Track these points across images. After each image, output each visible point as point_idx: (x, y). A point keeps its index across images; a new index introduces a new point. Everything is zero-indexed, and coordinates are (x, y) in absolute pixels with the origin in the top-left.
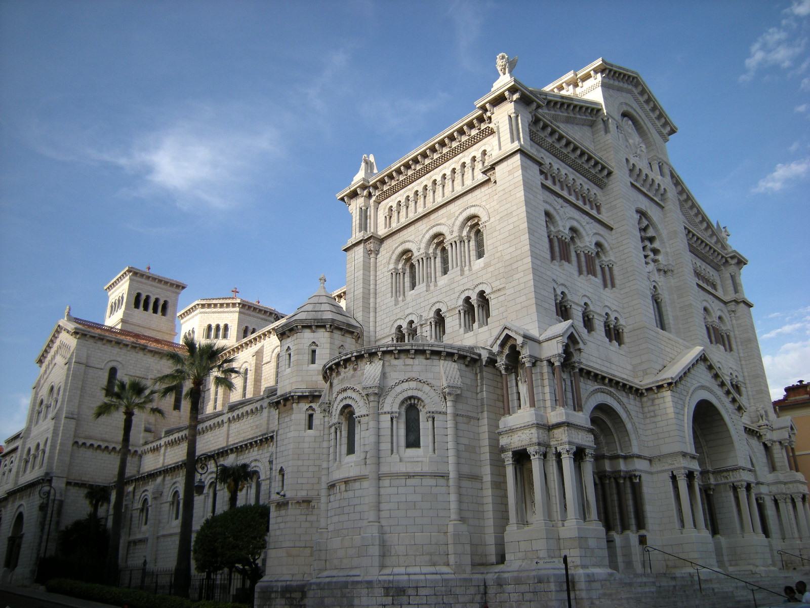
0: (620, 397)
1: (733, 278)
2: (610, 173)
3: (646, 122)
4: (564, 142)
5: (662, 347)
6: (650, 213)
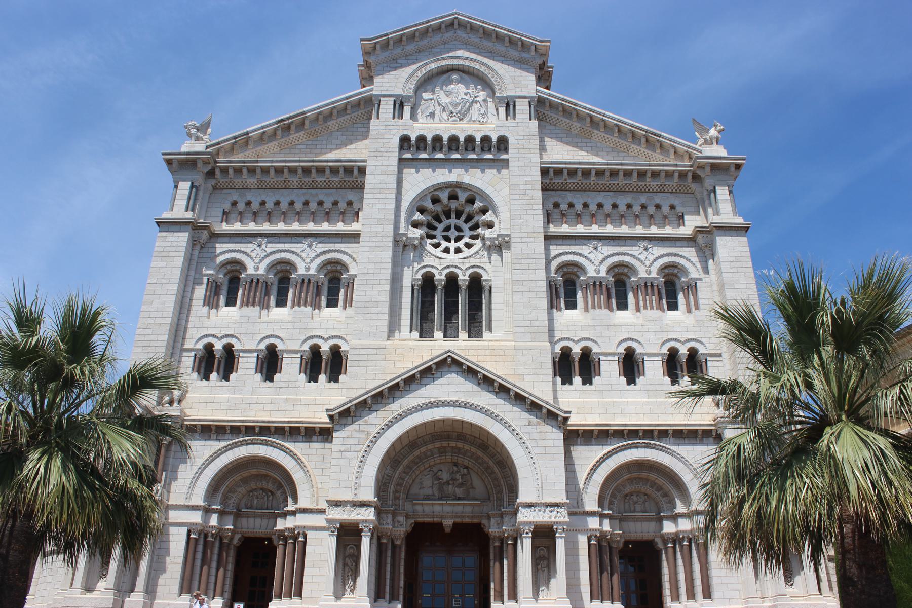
2: (362, 171)
4: (272, 172)
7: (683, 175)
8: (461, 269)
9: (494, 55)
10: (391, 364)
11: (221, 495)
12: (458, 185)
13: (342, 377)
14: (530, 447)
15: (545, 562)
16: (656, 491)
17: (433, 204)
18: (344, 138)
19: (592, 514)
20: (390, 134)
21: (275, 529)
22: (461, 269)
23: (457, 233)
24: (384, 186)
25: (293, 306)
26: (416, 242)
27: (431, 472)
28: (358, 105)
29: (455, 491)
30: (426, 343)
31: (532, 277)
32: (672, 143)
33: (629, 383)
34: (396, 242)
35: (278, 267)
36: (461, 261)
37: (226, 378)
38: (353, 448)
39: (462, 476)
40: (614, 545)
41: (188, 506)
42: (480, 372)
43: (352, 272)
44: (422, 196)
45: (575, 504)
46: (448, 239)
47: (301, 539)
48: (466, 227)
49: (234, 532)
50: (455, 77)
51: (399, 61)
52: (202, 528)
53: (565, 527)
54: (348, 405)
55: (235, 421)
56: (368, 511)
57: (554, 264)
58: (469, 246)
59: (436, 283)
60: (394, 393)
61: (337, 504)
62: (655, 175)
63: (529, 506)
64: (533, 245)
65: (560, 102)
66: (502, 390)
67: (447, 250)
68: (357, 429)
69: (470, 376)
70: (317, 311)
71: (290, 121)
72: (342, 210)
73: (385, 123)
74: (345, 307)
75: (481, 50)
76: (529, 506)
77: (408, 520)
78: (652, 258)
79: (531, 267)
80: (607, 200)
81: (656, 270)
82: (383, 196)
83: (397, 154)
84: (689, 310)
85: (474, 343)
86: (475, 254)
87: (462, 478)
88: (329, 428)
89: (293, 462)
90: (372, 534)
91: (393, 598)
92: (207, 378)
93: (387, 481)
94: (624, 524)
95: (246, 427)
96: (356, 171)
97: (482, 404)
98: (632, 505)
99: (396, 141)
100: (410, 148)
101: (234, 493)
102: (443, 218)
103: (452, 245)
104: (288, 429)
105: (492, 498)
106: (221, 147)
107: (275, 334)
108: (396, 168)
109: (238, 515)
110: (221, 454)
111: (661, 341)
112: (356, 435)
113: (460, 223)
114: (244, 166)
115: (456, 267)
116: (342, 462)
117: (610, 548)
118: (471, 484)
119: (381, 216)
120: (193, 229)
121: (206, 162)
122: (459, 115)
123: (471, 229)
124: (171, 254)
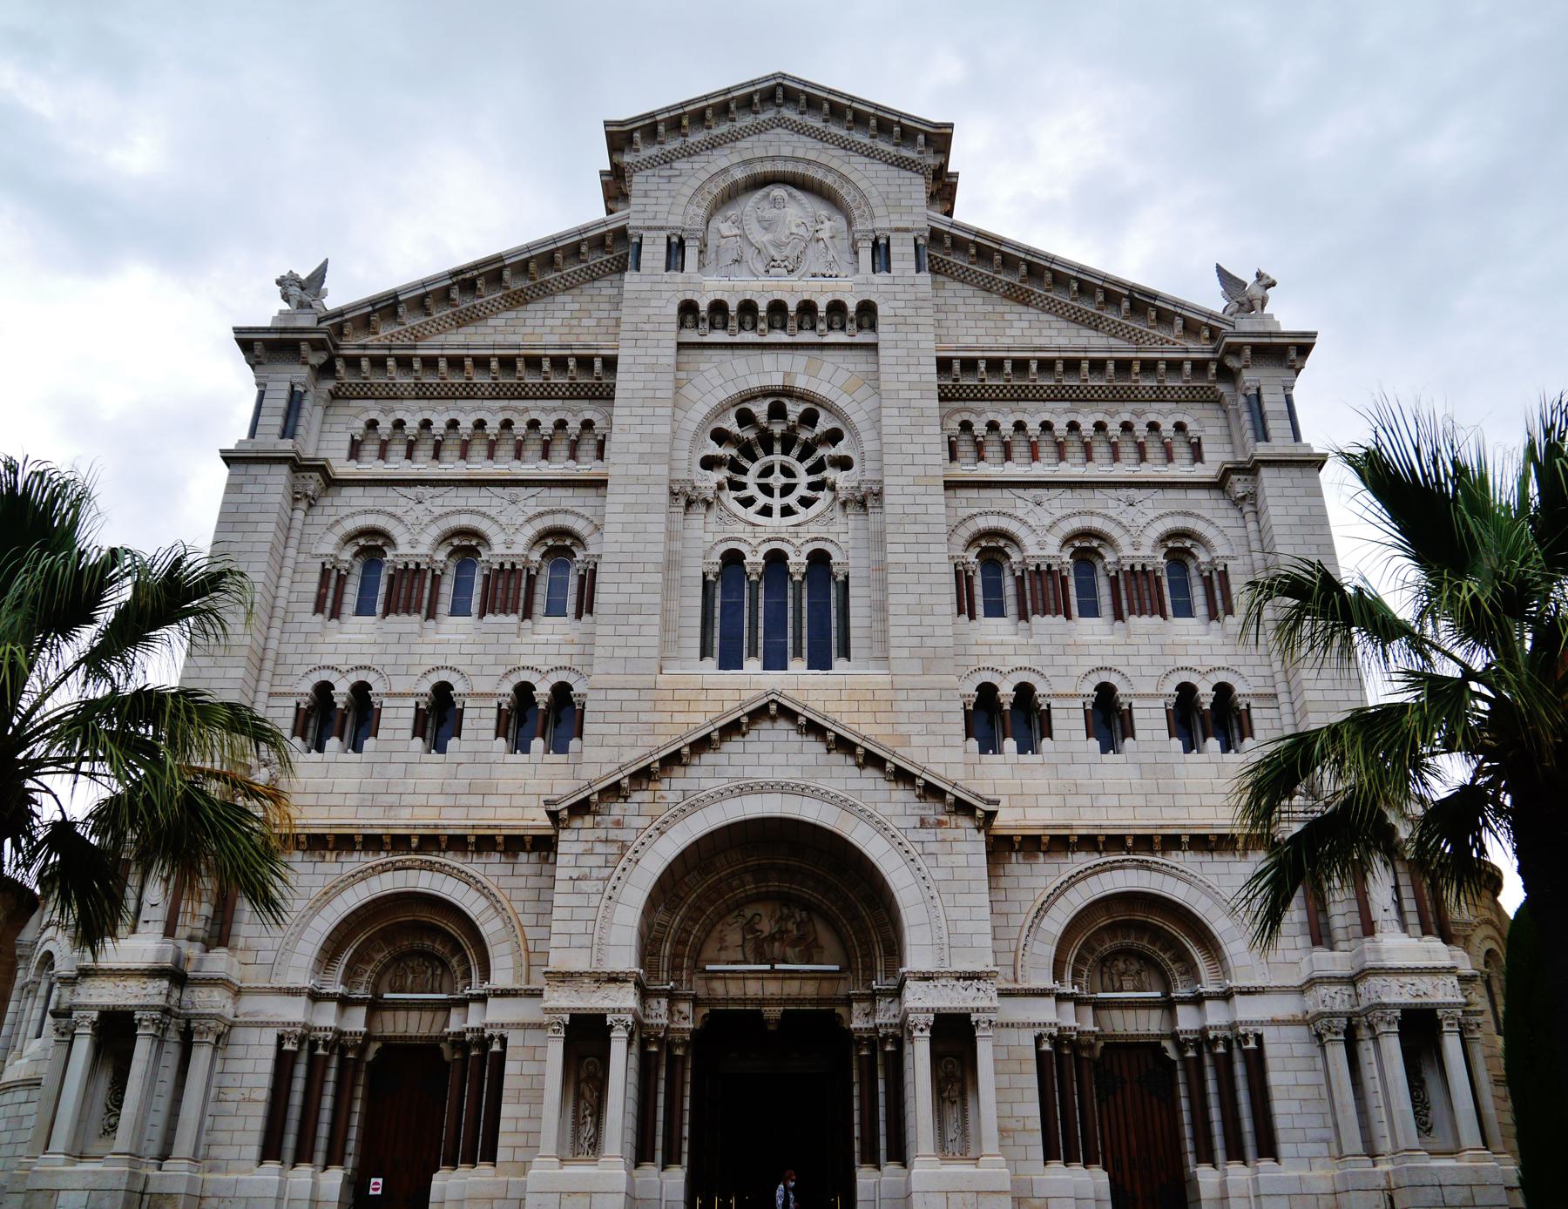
0: (463, 867)
1: (1256, 402)
2: (610, 364)
3: (834, 164)
5: (666, 717)
6: (801, 383)
7: (1200, 367)
8: (793, 544)
9: (850, 153)
10: (666, 717)
11: (343, 967)
12: (788, 392)
13: (574, 744)
14: (923, 866)
15: (957, 1087)
16: (1161, 950)
17: (740, 426)
18: (577, 306)
19: (1043, 993)
20: (661, 298)
21: (446, 1030)
22: (793, 544)
23: (784, 480)
24: (650, 394)
25: (482, 614)
26: (710, 496)
27: (740, 919)
28: (599, 243)
29: (784, 954)
30: (730, 676)
31: (924, 558)
32: (1179, 311)
33: (1104, 751)
34: (673, 493)
35: (456, 542)
36: (792, 529)
37: (357, 747)
38: (595, 873)
39: (799, 925)
40: (1085, 1054)
41: (280, 988)
42: (830, 730)
43: (592, 550)
44: (721, 411)
45: (1010, 976)
46: (767, 490)
47: (496, 1048)
48: (800, 468)
49: (368, 1038)
50: (778, 192)
51: (675, 165)
52: (305, 1032)
53: (993, 1017)
54: (586, 793)
55: (372, 826)
56: (623, 991)
57: (965, 533)
58: (806, 502)
59: (748, 569)
60: (672, 770)
61: (565, 977)
62: (1149, 366)
63: (926, 977)
64: (926, 500)
65: (972, 238)
66: (872, 760)
67: (766, 511)
68: (603, 837)
69: (812, 738)
70: (527, 623)
71: (475, 273)
72: (573, 437)
73: (654, 278)
74: (579, 616)
75: (827, 145)
76: (926, 977)
77: (698, 1009)
78: (1142, 521)
79: (922, 538)
80: (1059, 415)
81: (1151, 542)
82: (649, 411)
83: (673, 335)
84: (1213, 615)
85: (818, 676)
86: (818, 516)
87: (798, 930)
88: (550, 837)
89: (483, 903)
90: (631, 1034)
91: (670, 1159)
92: (320, 748)
93: (659, 936)
94: (1103, 1014)
95: (393, 836)
96: (598, 364)
97: (833, 786)
98: (1115, 978)
99: (673, 310)
100: (697, 326)
101: (369, 963)
102: (759, 451)
103: (777, 503)
104: (473, 839)
105: (854, 966)
106: (346, 321)
107: (449, 664)
108: (672, 361)
109: (375, 1006)
110: (343, 889)
111: (1161, 672)
112: (599, 848)
113: (791, 460)
114: (390, 356)
115: (783, 540)
116: (575, 900)
117: (1079, 1060)
118: (816, 939)
119: (646, 448)
120: (294, 472)
121: (317, 346)
122: (786, 263)
123: (810, 471)
124: (252, 517)
